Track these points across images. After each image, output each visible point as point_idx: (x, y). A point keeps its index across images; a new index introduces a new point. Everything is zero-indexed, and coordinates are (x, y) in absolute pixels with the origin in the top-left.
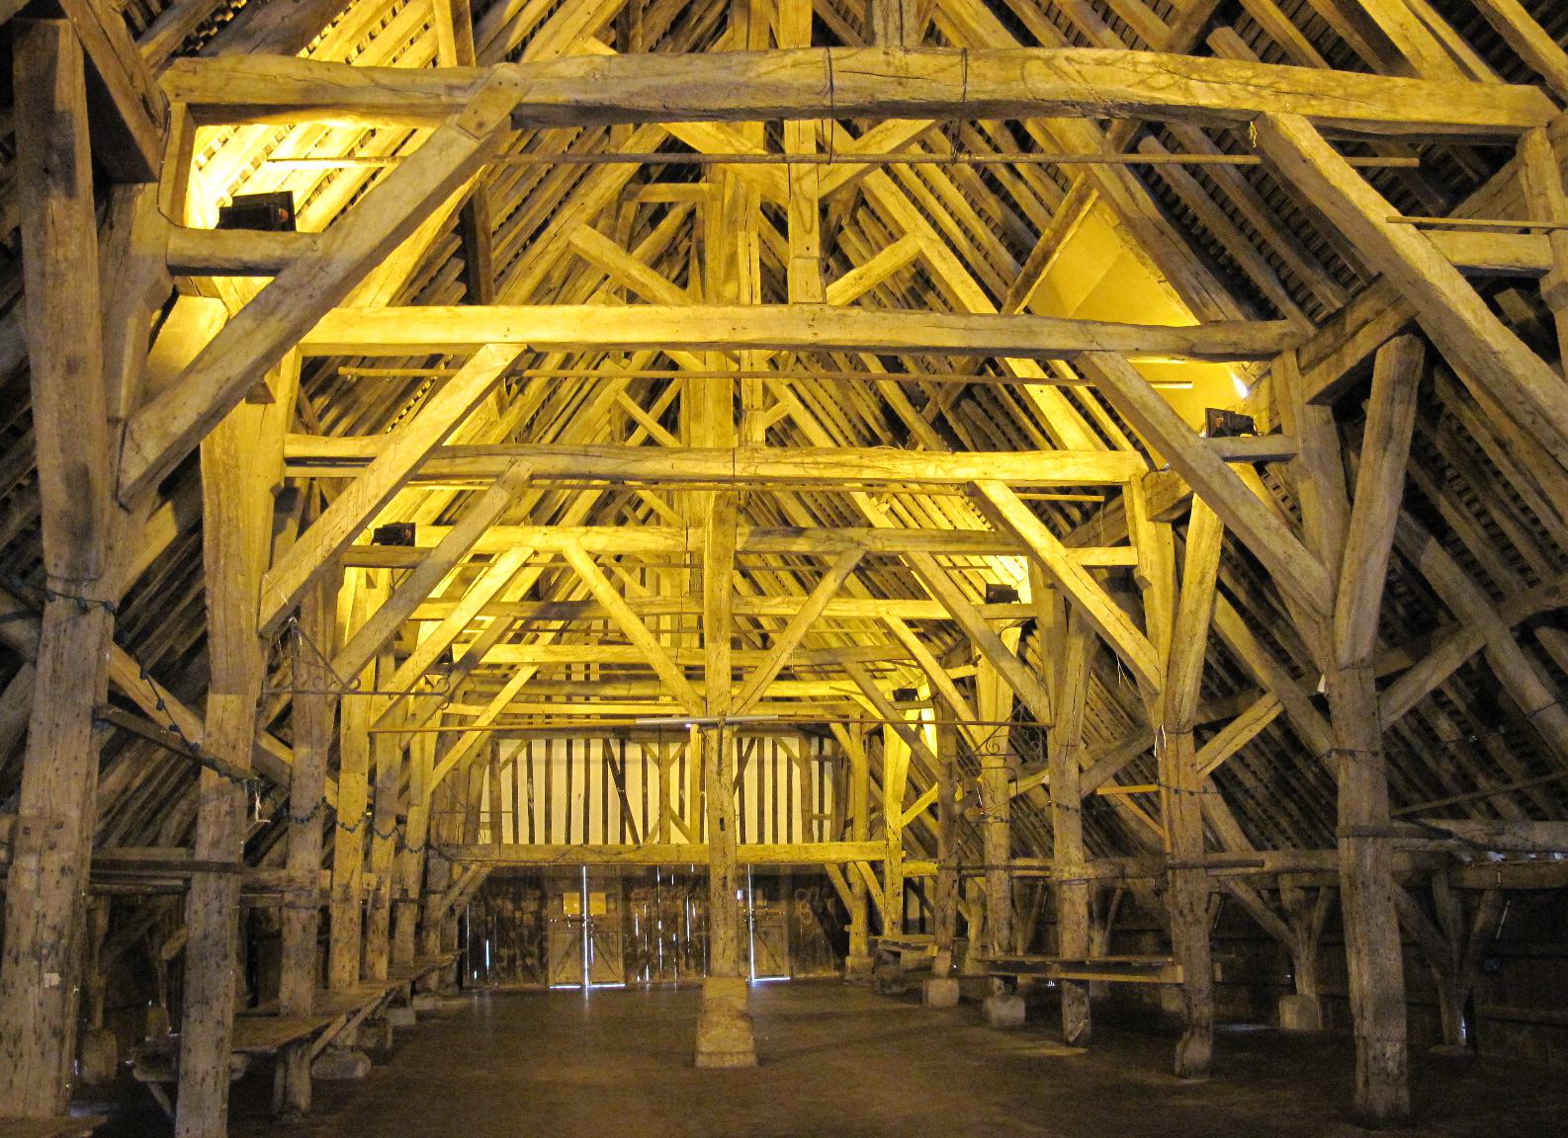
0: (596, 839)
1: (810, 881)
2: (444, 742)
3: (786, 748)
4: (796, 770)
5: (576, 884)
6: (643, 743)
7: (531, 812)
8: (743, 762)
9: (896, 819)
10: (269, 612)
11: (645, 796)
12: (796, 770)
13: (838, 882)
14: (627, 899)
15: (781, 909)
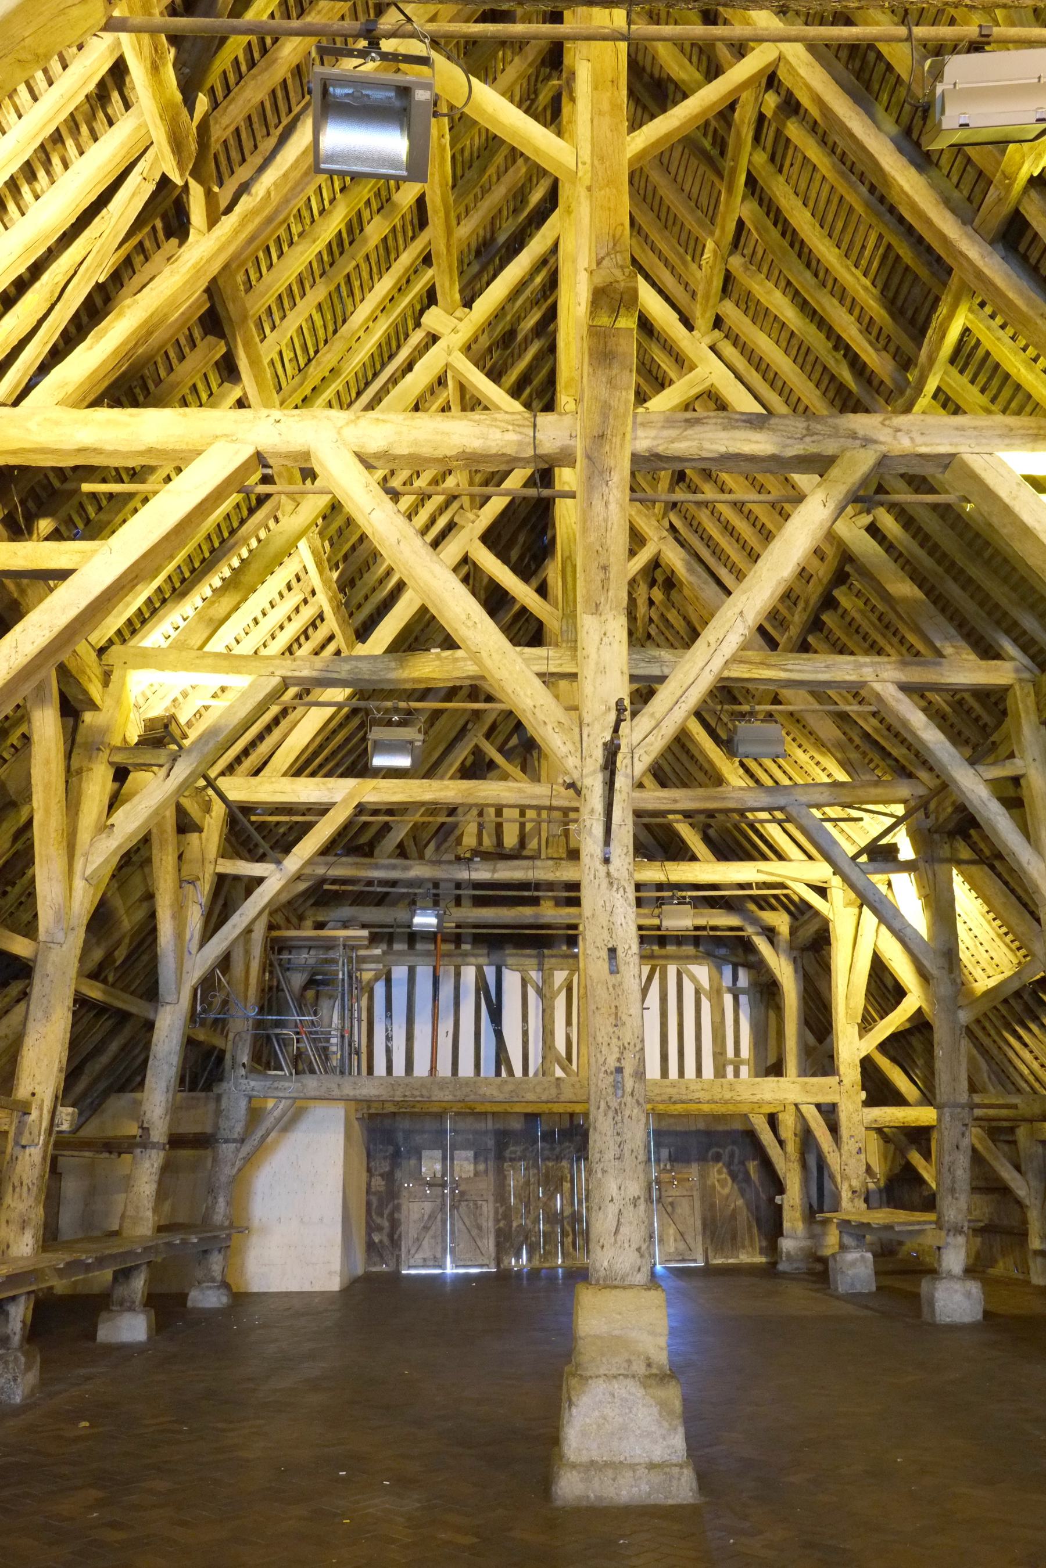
3: (693, 979)
4: (706, 1005)
7: (389, 1051)
11: (525, 1033)
12: (706, 1005)
13: (766, 1137)
15: (693, 1171)
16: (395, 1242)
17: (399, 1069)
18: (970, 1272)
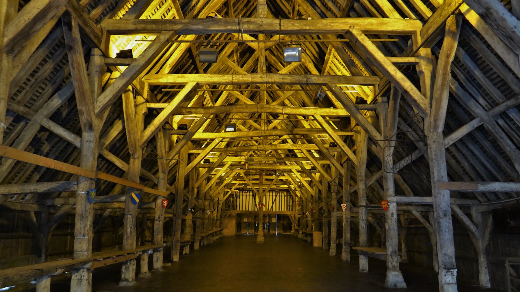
1: (286, 217)
2: (225, 195)
8: (276, 196)
10: (205, 191)
12: (286, 197)
13: (290, 218)
14: (255, 220)
16: (241, 230)
17: (241, 209)
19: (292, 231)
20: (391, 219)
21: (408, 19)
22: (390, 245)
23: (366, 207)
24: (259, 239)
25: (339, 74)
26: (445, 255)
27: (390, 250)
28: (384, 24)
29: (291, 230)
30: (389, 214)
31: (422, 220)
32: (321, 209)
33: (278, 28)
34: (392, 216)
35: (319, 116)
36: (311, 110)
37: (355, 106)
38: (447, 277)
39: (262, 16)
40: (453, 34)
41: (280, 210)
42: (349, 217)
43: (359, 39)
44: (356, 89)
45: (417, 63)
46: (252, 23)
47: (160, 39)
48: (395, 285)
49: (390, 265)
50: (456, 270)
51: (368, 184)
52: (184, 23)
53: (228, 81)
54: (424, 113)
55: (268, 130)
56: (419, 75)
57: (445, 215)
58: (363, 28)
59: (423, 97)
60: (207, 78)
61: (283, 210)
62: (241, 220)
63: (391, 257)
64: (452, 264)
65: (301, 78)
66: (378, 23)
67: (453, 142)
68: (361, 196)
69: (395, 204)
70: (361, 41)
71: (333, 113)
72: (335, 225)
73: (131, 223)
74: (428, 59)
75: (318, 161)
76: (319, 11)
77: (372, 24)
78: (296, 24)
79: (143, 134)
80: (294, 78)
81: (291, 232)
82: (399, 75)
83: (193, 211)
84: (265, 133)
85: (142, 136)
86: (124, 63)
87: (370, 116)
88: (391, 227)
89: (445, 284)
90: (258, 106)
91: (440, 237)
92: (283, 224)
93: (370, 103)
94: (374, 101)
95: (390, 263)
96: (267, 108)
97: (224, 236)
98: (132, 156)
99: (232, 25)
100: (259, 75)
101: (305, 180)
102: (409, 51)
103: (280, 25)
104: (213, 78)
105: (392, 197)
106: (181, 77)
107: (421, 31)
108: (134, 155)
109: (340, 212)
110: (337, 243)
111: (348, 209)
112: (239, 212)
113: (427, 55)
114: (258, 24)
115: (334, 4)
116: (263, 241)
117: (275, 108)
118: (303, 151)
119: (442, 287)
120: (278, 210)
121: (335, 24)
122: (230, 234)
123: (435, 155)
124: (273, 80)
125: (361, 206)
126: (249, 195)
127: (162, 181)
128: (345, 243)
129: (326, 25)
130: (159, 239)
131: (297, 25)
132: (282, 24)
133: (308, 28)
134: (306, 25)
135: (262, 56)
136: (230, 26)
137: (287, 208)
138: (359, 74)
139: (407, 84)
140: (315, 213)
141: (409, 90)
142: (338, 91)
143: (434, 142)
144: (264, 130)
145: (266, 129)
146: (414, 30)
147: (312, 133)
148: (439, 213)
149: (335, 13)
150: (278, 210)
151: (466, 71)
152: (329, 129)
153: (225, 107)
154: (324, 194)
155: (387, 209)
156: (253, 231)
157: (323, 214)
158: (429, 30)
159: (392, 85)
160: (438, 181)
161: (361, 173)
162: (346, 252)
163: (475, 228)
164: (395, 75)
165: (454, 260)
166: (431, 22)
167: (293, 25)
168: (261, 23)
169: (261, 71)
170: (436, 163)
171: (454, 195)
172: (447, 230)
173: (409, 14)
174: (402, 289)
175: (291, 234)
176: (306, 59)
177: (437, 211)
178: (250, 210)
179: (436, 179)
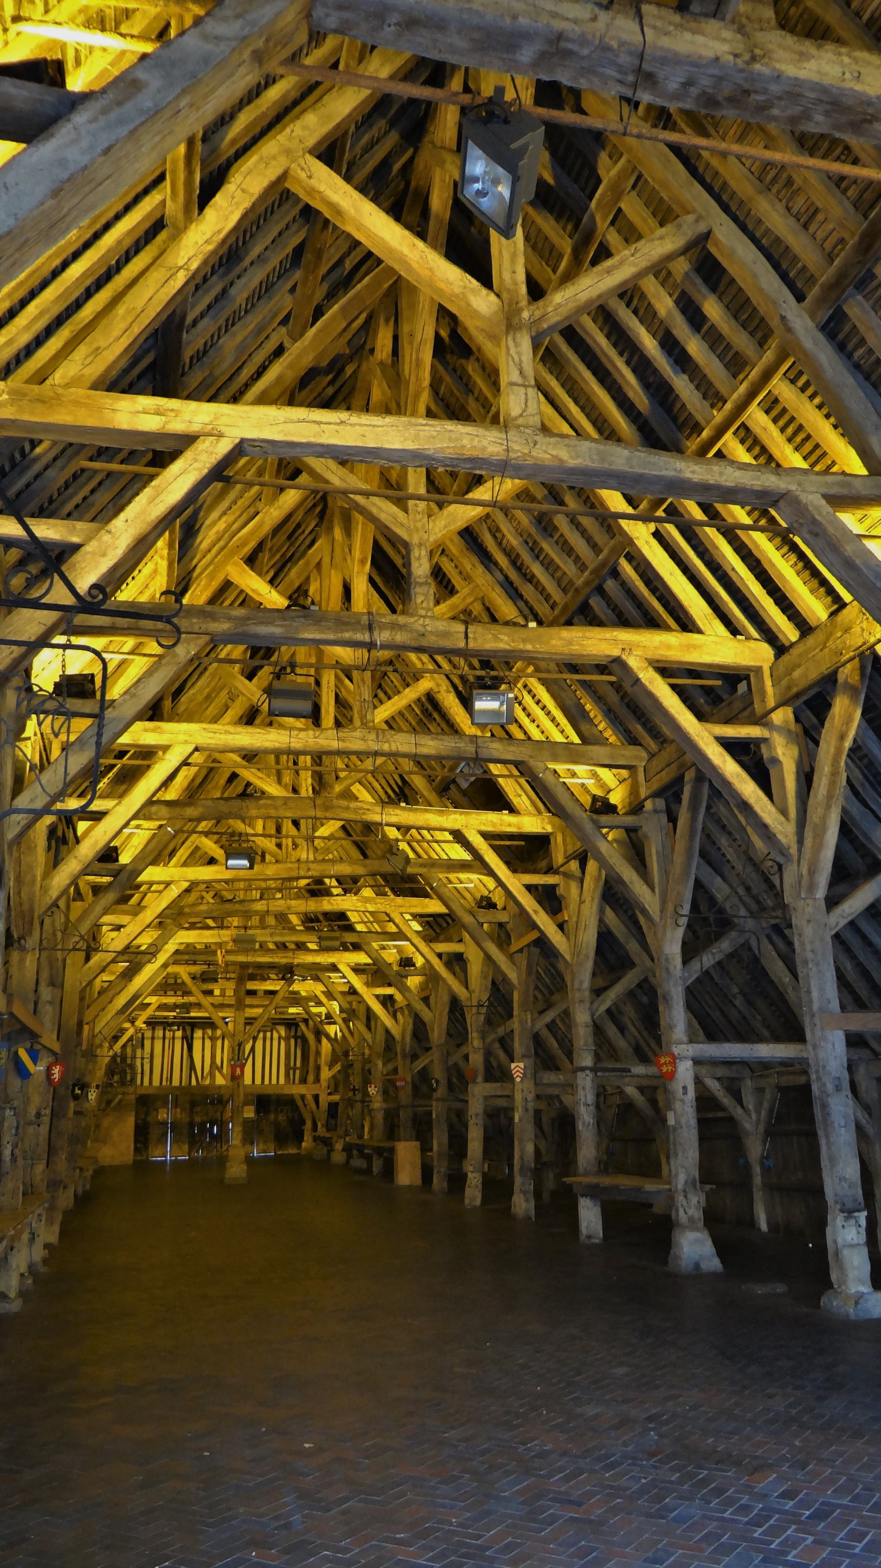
0: (176, 1082)
1: (287, 1102)
3: (278, 1032)
5: (165, 1104)
6: (204, 1029)
9: (326, 1074)
11: (203, 1056)
12: (283, 1043)
13: (300, 1103)
14: (191, 1112)
16: (146, 1148)
18: (343, 1150)
19: (304, 1144)
20: (682, 1101)
21: (743, 638)
22: (682, 1167)
23: (594, 1070)
24: (234, 1169)
25: (559, 738)
26: (842, 1179)
27: (681, 1180)
28: (695, 647)
29: (301, 1139)
30: (677, 1086)
31: (726, 1101)
32: (424, 1075)
33: (462, 644)
34: (685, 1093)
35: (474, 832)
36: (452, 817)
37: (592, 820)
38: (846, 1230)
39: (423, 612)
40: (853, 691)
41: (267, 1082)
42: (531, 1097)
43: (643, 681)
44: (579, 774)
45: (765, 740)
46: (401, 627)
47: (175, 655)
48: (697, 1266)
49: (683, 1217)
50: (865, 1213)
51: (597, 1010)
52: (236, 618)
53: (277, 745)
54: (783, 855)
55: (315, 861)
56: (769, 766)
57: (838, 1088)
58: (650, 655)
59: (783, 819)
60: (222, 736)
61: (274, 1081)
62: (147, 1113)
63: (685, 1196)
64: (855, 1200)
65: (462, 745)
66: (681, 646)
67: (846, 921)
68: (582, 1042)
69: (689, 1063)
70: (647, 683)
71: (510, 825)
72: (481, 1122)
73: (14, 1131)
74: (789, 731)
75: (433, 945)
76: (501, 578)
77: (669, 647)
78: (502, 637)
79: (46, 882)
80: (446, 743)
81: (300, 1147)
82: (729, 767)
83: (78, 1091)
84: (309, 869)
85: (45, 889)
86: (82, 711)
87: (615, 840)
88: (683, 1121)
89: (844, 1246)
90: (319, 801)
91: (827, 1137)
92: (276, 1123)
93: (626, 814)
94: (636, 808)
95: (681, 1212)
96: (340, 807)
97: (102, 1167)
98: (16, 945)
99: (355, 630)
100: (357, 734)
101: (377, 997)
102: (738, 705)
103: (466, 637)
104: (237, 736)
105: (684, 1046)
106: (154, 730)
107: (771, 668)
108: (23, 942)
109: (510, 1085)
110: (486, 1169)
111: (529, 1076)
112: (143, 1092)
113: (786, 722)
114: (417, 631)
115: (547, 569)
116: (244, 1175)
117: (361, 809)
118: (393, 915)
119: (837, 1253)
120: (258, 1081)
121: (590, 642)
122: (117, 1162)
123: (812, 951)
124: (394, 748)
125: (583, 1069)
126: (174, 1038)
127: (49, 1008)
128: (522, 1169)
129: (570, 642)
130: (39, 1178)
131: (506, 638)
132: (470, 635)
133: (529, 647)
134: (524, 641)
135: (364, 683)
136: (348, 631)
137: (287, 1075)
138: (601, 741)
139: (748, 789)
140: (403, 1088)
141: (752, 801)
142: (549, 779)
143: (809, 921)
144: (307, 861)
145: (311, 857)
146: (758, 664)
147: (433, 870)
148: (824, 1084)
149: (544, 589)
150: (258, 1081)
151: (865, 761)
152: (500, 868)
153: (229, 803)
154: (437, 1034)
155: (671, 1075)
156: (186, 1147)
157: (435, 1090)
158: (793, 669)
159: (690, 775)
160: (821, 1010)
161: (581, 983)
162: (525, 1193)
163: (867, 1116)
164: (721, 765)
165: (860, 1191)
166: (800, 655)
167: (496, 638)
168: (421, 629)
169: (362, 723)
170: (814, 969)
171: (854, 1041)
172: (843, 1123)
173: (744, 627)
174: (714, 1275)
175: (303, 1152)
176: (440, 682)
177: (819, 1078)
178: (176, 1082)
179: (815, 1007)
